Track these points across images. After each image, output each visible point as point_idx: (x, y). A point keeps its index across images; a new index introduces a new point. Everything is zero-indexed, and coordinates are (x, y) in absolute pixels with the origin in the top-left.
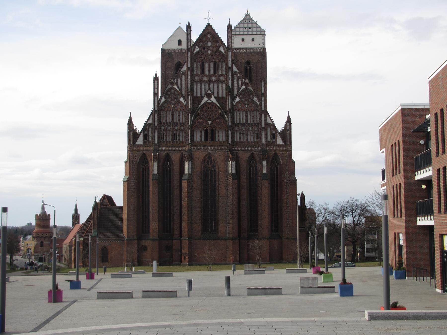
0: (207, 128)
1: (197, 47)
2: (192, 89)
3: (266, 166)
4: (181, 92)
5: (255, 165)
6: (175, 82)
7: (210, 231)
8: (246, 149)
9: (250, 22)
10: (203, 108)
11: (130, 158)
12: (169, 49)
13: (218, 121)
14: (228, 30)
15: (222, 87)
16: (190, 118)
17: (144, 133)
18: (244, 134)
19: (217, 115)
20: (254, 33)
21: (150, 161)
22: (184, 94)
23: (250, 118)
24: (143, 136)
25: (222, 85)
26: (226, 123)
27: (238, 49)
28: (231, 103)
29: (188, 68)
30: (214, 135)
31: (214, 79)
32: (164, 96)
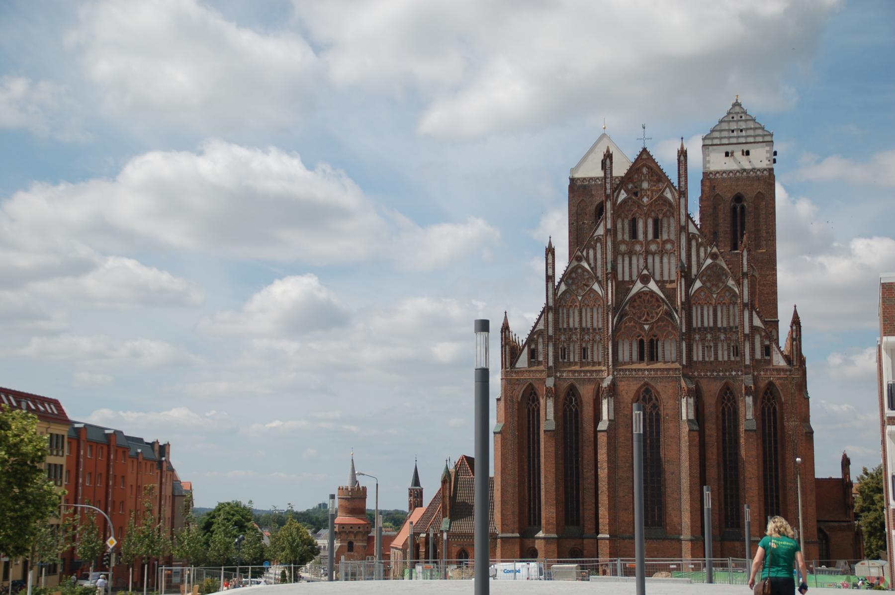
0: (641, 337)
1: (622, 191)
2: (614, 268)
3: (752, 406)
4: (595, 274)
5: (732, 404)
6: (583, 255)
7: (650, 523)
8: (715, 374)
9: (742, 119)
10: (633, 302)
11: (505, 392)
12: (584, 179)
13: (663, 324)
14: (679, 160)
15: (669, 263)
16: (610, 320)
17: (529, 347)
18: (711, 347)
19: (660, 314)
20: (751, 140)
22: (600, 277)
23: (722, 318)
24: (528, 353)
25: (669, 259)
26: (674, 327)
28: (685, 290)
29: (607, 231)
30: (655, 350)
31: (653, 247)
32: (564, 281)
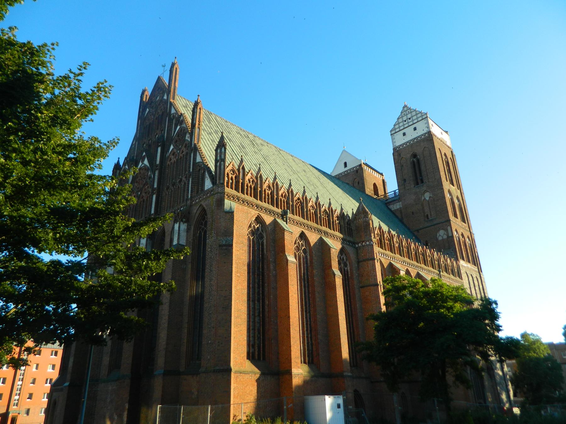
27: (400, 145)
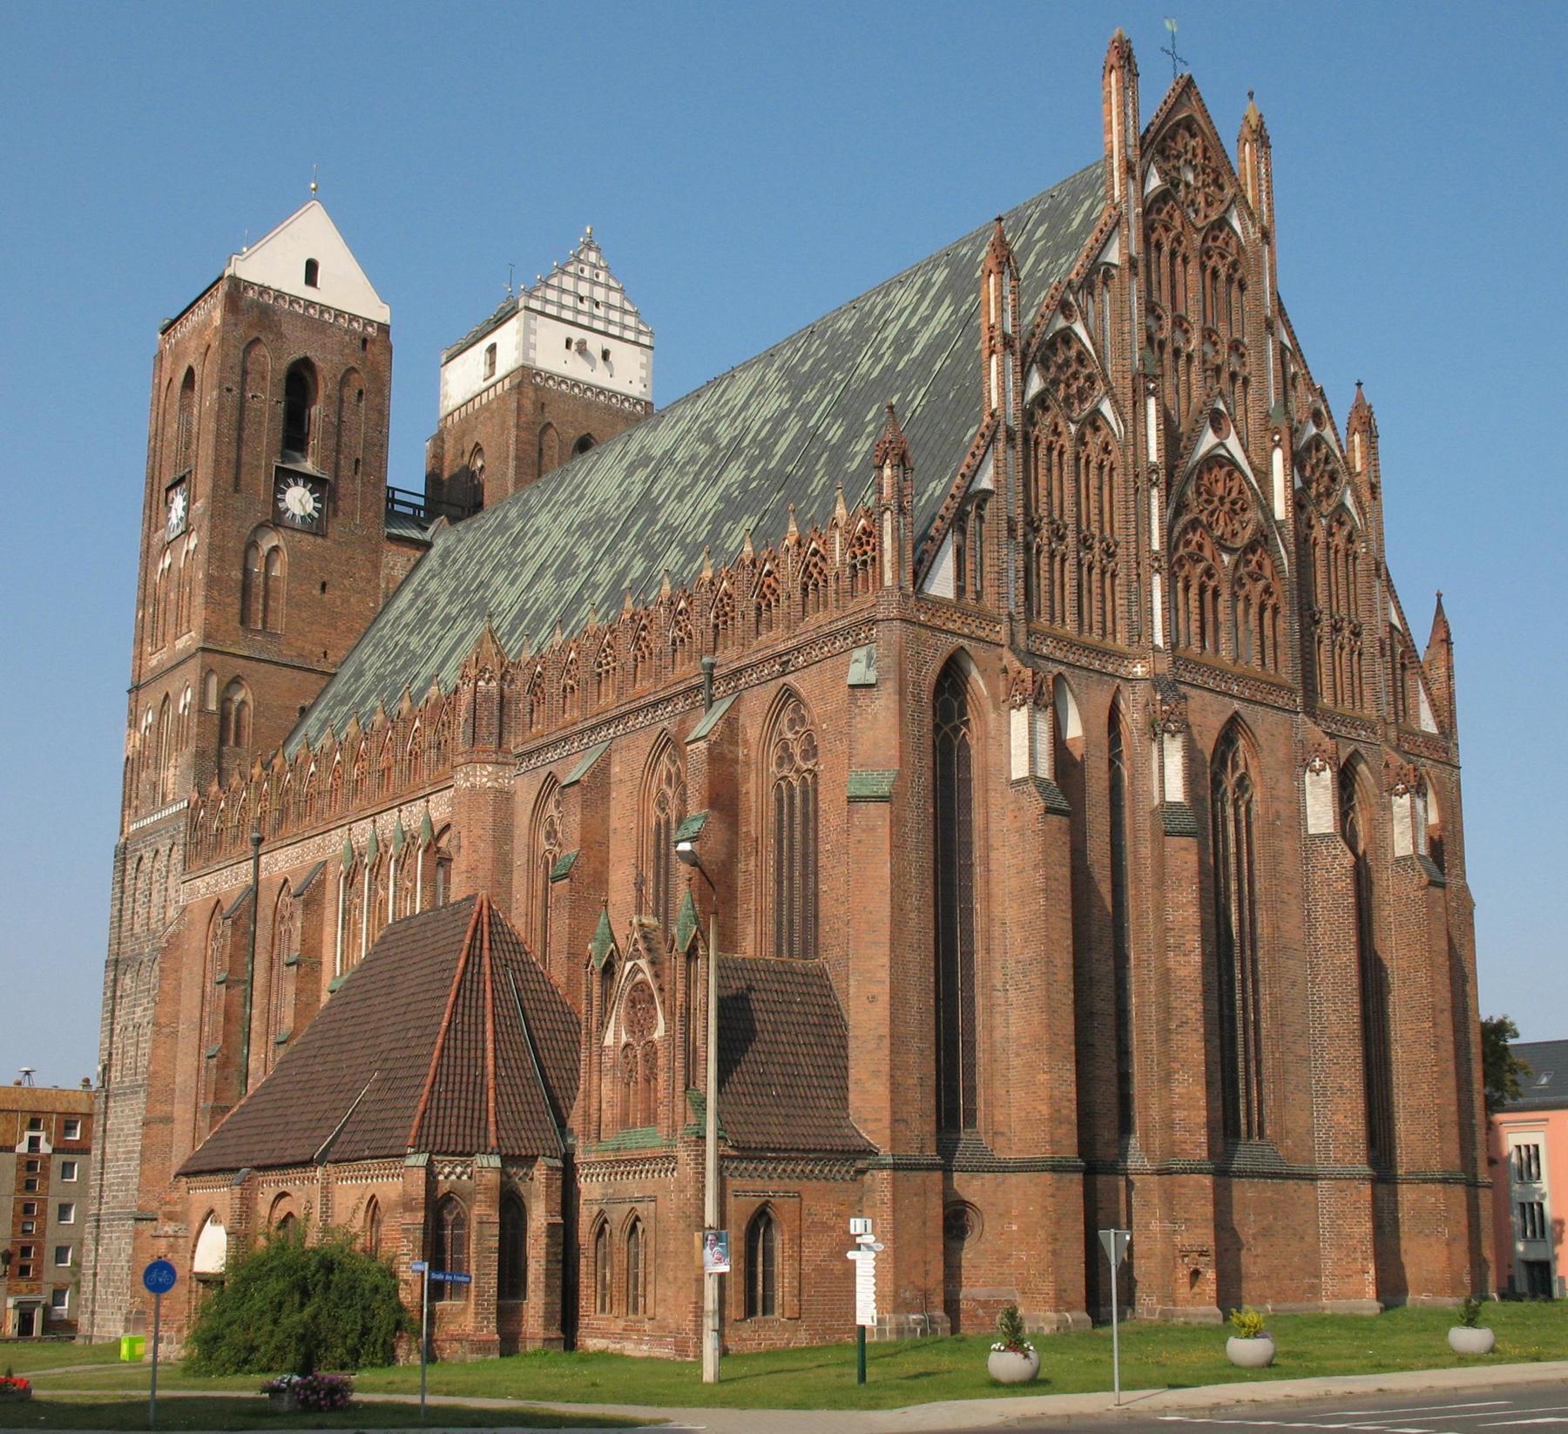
21: (988, 705)
27: (551, 377)
